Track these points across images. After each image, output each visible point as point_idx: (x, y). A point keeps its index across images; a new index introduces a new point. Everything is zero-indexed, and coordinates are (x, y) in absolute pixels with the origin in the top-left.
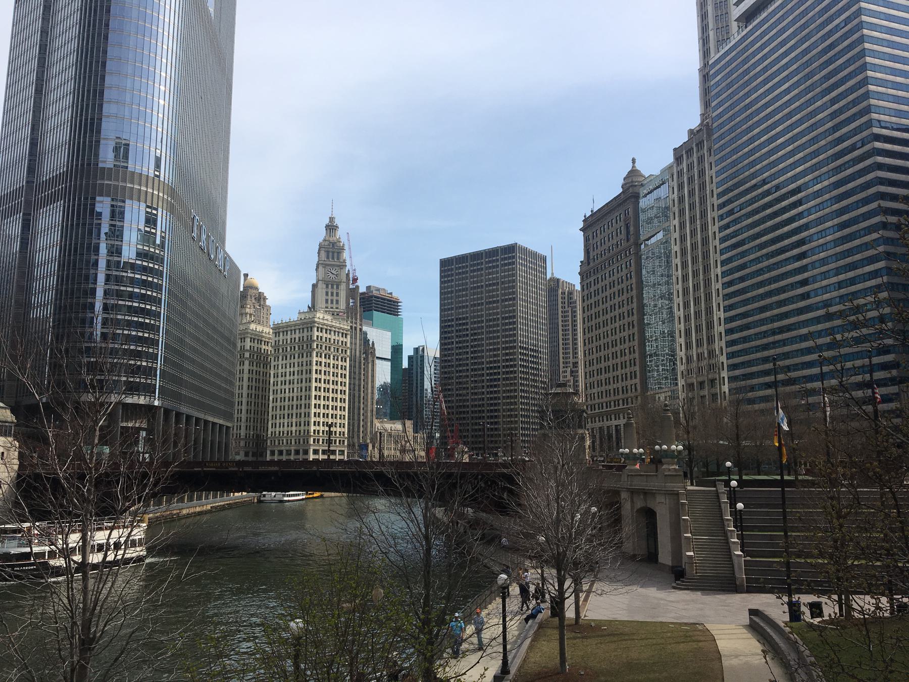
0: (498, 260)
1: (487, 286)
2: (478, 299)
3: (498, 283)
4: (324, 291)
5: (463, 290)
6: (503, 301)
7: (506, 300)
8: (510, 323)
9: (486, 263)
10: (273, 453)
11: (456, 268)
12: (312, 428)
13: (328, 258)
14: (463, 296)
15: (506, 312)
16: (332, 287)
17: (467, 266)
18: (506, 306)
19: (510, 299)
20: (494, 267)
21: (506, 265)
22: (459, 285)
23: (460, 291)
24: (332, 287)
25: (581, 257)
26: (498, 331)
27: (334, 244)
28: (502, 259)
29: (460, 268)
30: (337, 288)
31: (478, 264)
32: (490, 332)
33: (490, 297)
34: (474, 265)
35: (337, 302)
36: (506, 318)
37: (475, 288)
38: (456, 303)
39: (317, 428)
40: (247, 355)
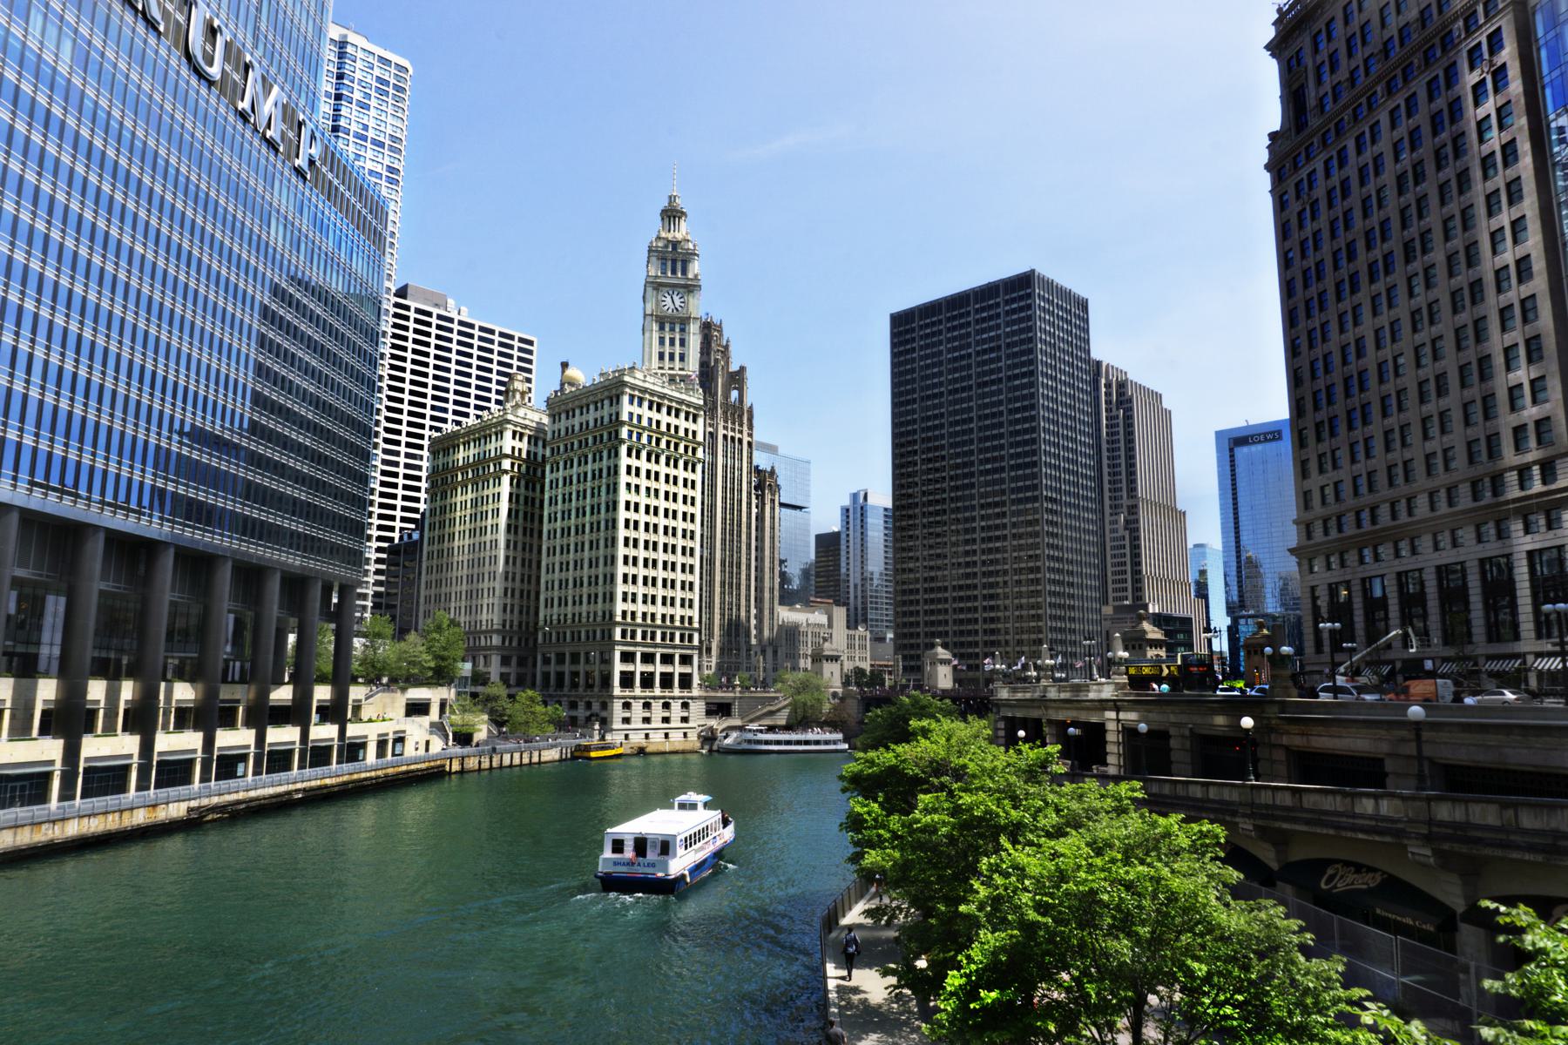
0: (998, 305)
1: (978, 353)
2: (963, 379)
3: (999, 347)
4: (656, 336)
5: (934, 365)
6: (1009, 378)
7: (1016, 377)
8: (1025, 420)
9: (977, 311)
10: (547, 661)
11: (921, 327)
12: (620, 606)
13: (664, 273)
14: (934, 375)
15: (1016, 399)
16: (672, 330)
17: (940, 322)
19: (1024, 375)
20: (991, 318)
22: (927, 357)
23: (928, 367)
24: (672, 330)
25: (1272, 116)
26: (1001, 436)
27: (675, 244)
29: (927, 326)
30: (682, 330)
32: (987, 439)
33: (985, 373)
35: (682, 358)
36: (1017, 410)
39: (630, 607)
40: (506, 464)
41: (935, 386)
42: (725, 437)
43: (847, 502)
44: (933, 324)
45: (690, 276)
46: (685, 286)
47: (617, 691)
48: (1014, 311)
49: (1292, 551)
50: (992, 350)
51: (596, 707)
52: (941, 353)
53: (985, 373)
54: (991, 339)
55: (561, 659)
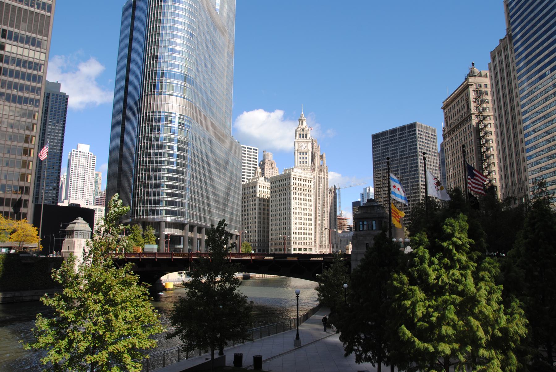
1: (400, 148)
2: (395, 157)
3: (406, 147)
4: (299, 156)
7: (412, 156)
10: (272, 250)
13: (300, 137)
15: (412, 164)
18: (412, 160)
20: (403, 137)
21: (411, 135)
22: (384, 149)
23: (384, 152)
28: (408, 132)
30: (306, 154)
31: (394, 136)
33: (402, 155)
34: (392, 137)
35: (306, 162)
36: (412, 167)
37: (393, 150)
42: (319, 177)
43: (362, 192)
45: (308, 138)
50: (404, 147)
52: (388, 148)
53: (402, 155)
54: (404, 144)
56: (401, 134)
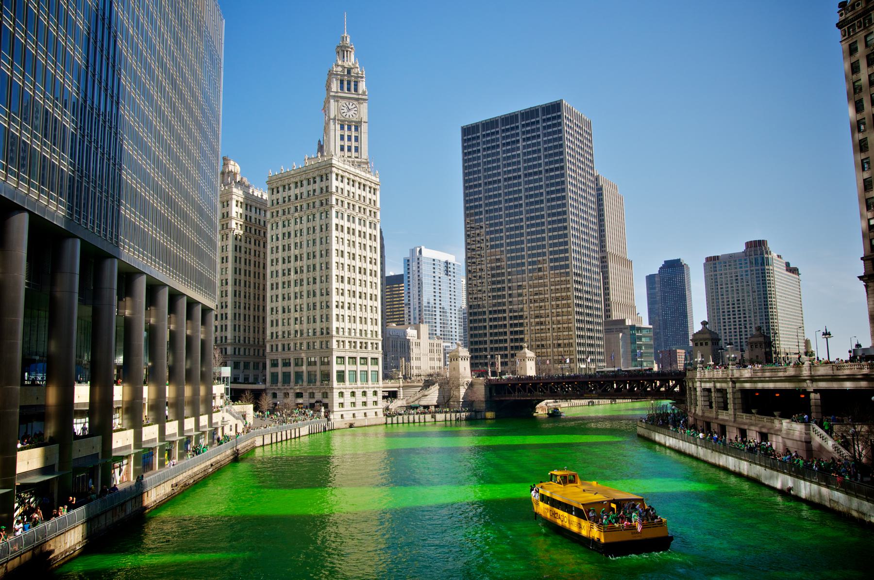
0: (538, 122)
3: (539, 150)
7: (552, 170)
8: (558, 199)
10: (275, 364)
11: (484, 136)
13: (342, 88)
14: (494, 168)
15: (552, 185)
16: (349, 129)
19: (557, 169)
20: (533, 131)
22: (488, 156)
24: (349, 129)
36: (552, 192)
38: (485, 177)
41: (495, 175)
43: (408, 255)
44: (493, 134)
45: (360, 92)
46: (357, 99)
47: (335, 384)
48: (549, 127)
49: (860, 278)
50: (534, 152)
51: (318, 396)
52: (498, 153)
55: (286, 364)
56: (528, 125)
